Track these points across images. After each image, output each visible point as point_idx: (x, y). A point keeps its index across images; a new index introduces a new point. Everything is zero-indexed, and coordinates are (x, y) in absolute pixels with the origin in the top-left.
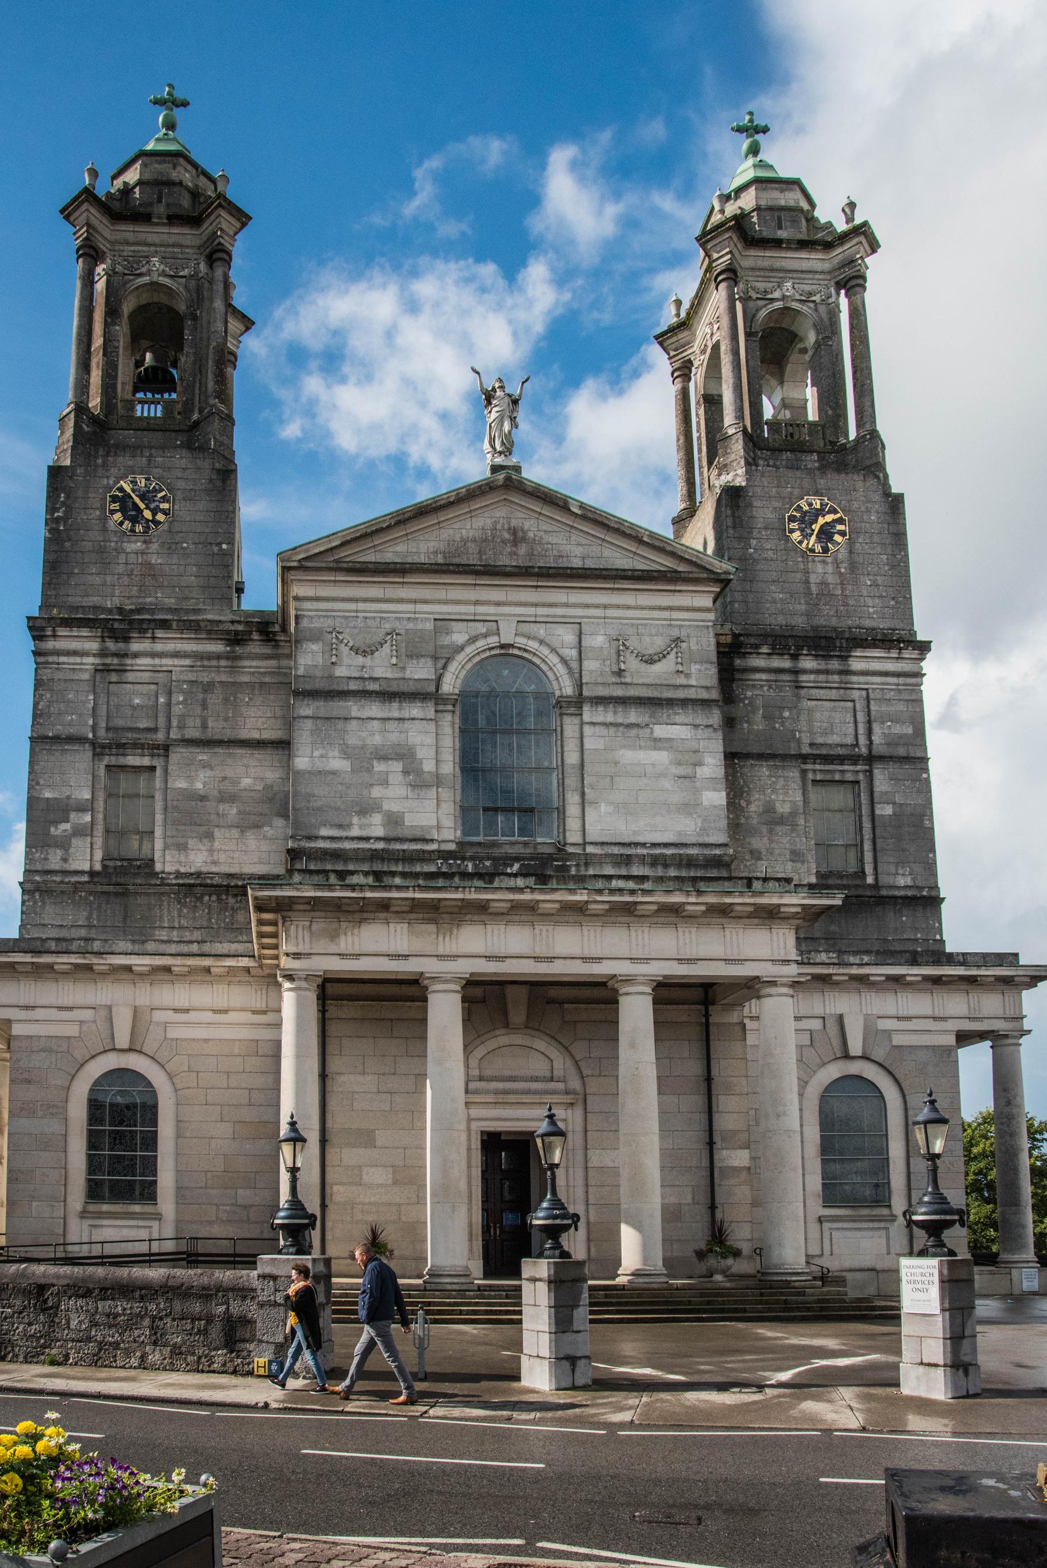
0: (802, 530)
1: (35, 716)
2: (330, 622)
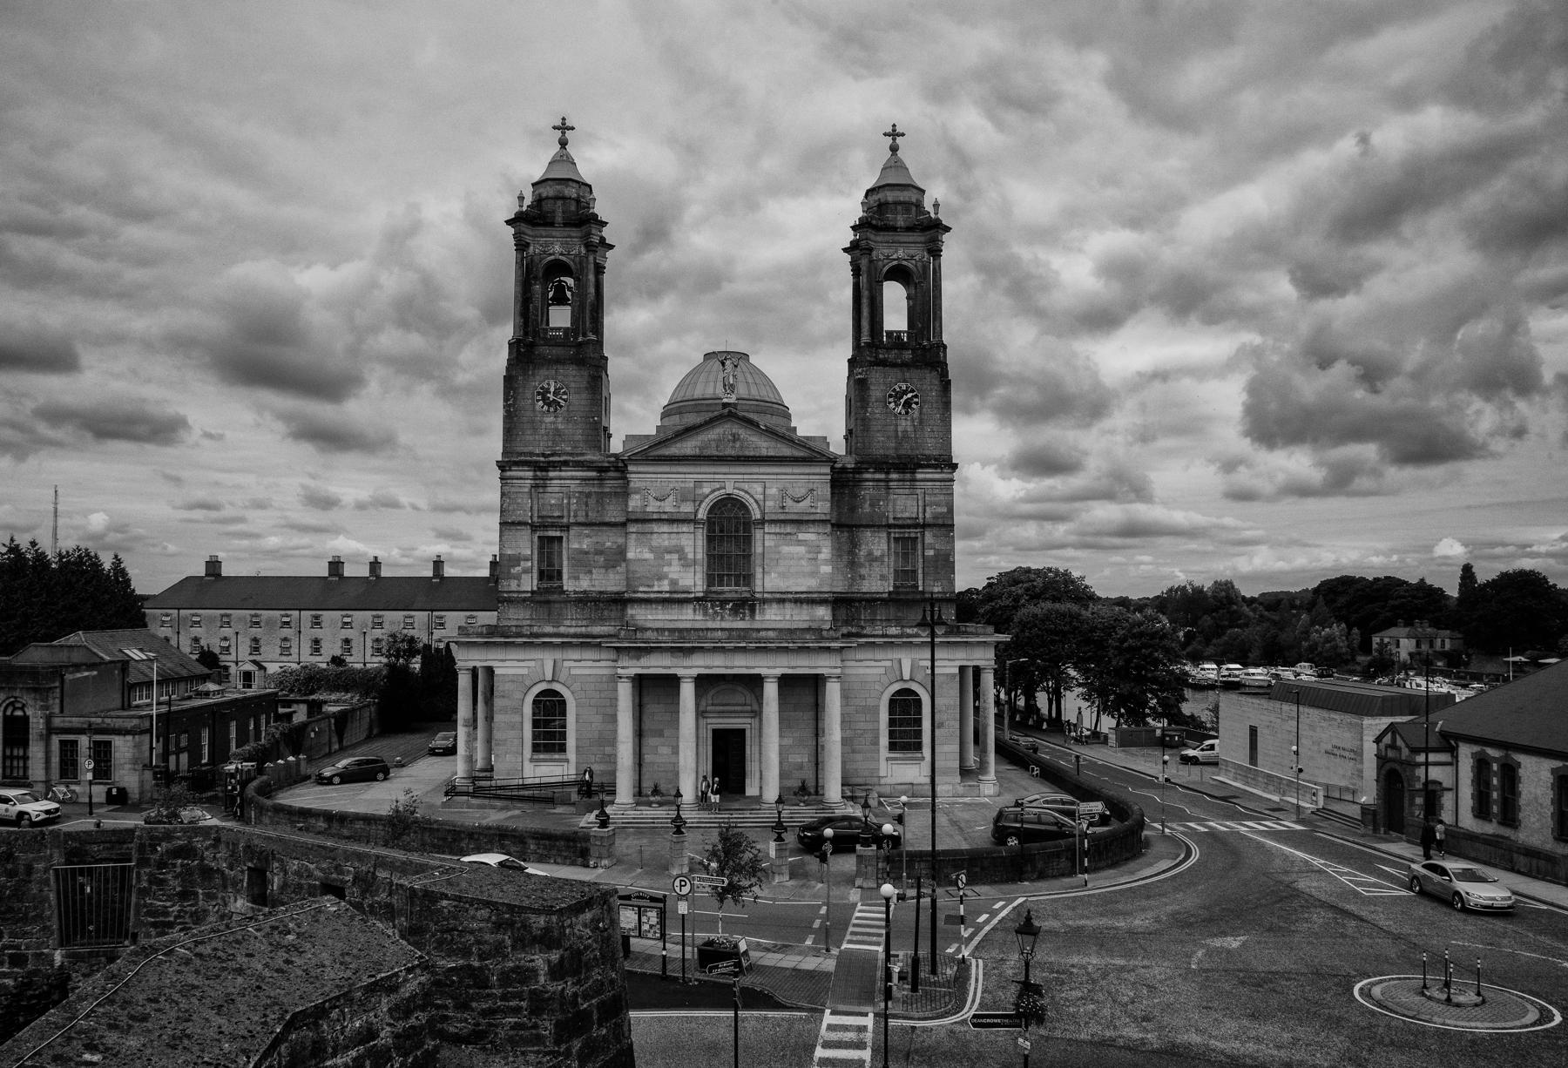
0: (895, 402)
1: (501, 512)
2: (644, 484)
